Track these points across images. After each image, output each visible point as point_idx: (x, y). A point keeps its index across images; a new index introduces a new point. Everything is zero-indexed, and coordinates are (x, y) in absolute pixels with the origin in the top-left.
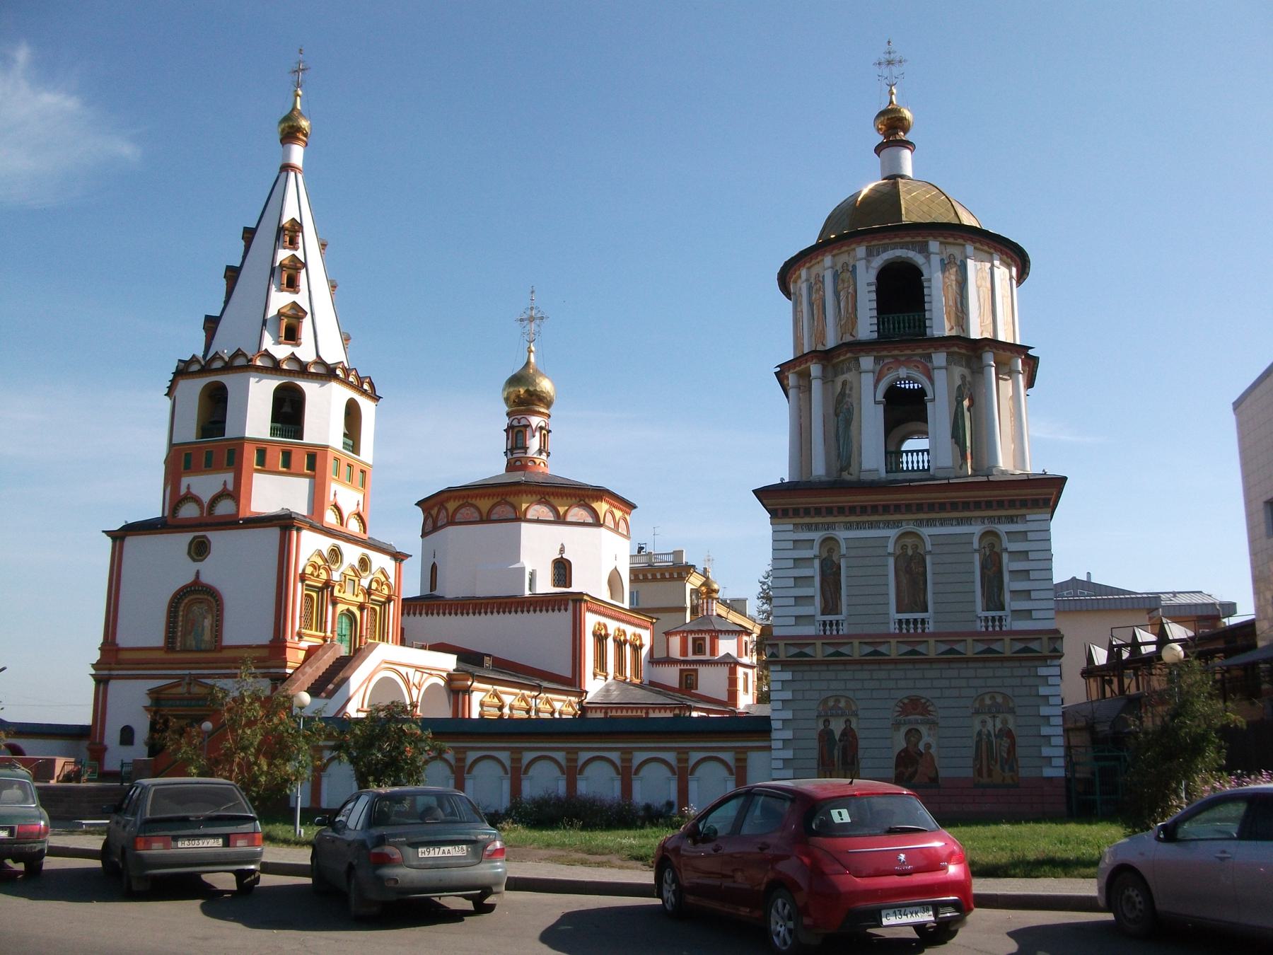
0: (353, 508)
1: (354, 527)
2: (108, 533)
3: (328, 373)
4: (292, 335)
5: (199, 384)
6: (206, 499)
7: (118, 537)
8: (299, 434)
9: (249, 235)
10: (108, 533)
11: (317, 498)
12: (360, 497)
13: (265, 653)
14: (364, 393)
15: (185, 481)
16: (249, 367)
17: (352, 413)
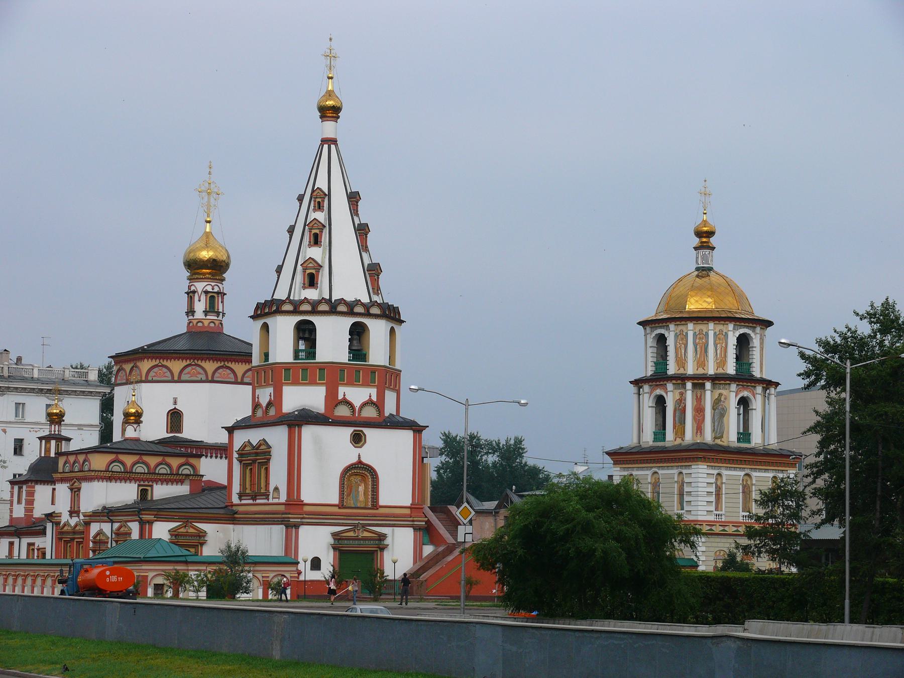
0: (366, 398)
1: (370, 413)
2: (226, 428)
3: (333, 308)
4: (312, 281)
5: (259, 323)
6: (264, 405)
7: (230, 430)
8: (314, 357)
9: (301, 199)
10: (226, 428)
11: (332, 400)
12: (373, 392)
13: (282, 508)
14: (368, 315)
15: (258, 392)
16: (279, 312)
17: (358, 332)
